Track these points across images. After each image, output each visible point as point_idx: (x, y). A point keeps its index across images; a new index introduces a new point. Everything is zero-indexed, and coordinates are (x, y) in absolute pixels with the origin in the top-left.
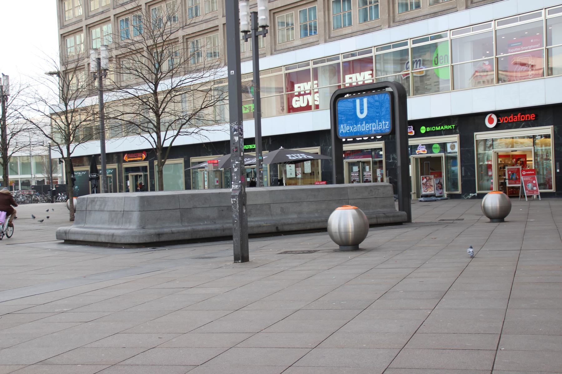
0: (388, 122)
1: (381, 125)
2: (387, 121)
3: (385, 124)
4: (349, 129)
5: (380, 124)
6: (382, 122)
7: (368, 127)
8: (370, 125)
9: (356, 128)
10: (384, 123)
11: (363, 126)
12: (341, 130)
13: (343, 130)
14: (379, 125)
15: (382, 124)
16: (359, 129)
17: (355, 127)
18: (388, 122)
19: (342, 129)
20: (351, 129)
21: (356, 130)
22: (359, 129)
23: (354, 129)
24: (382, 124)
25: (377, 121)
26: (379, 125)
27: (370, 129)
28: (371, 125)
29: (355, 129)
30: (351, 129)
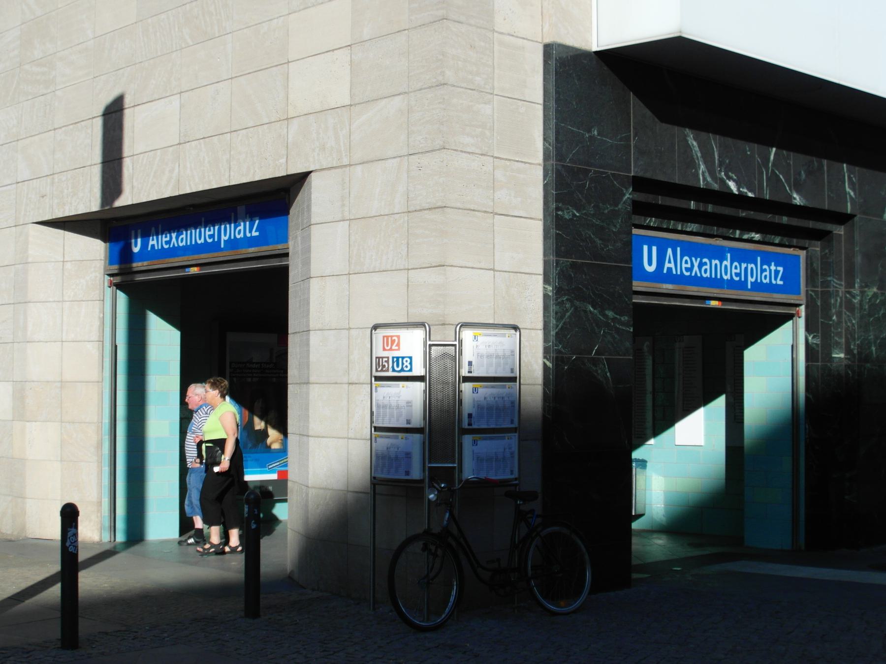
0: (781, 269)
1: (767, 273)
2: (780, 266)
3: (777, 272)
4: (689, 266)
5: (765, 270)
6: (769, 266)
7: (738, 271)
8: (744, 266)
9: (708, 267)
10: (773, 268)
11: (726, 267)
12: (667, 265)
13: (672, 265)
14: (763, 271)
15: (770, 271)
16: (200, 232)
17: (705, 264)
18: (781, 269)
19: (670, 262)
20: (696, 268)
21: (708, 275)
22: (200, 232)
23: (704, 268)
24: (770, 271)
25: (759, 259)
26: (763, 271)
27: (216, 240)
28: (746, 269)
29: (706, 271)
30: (696, 268)
